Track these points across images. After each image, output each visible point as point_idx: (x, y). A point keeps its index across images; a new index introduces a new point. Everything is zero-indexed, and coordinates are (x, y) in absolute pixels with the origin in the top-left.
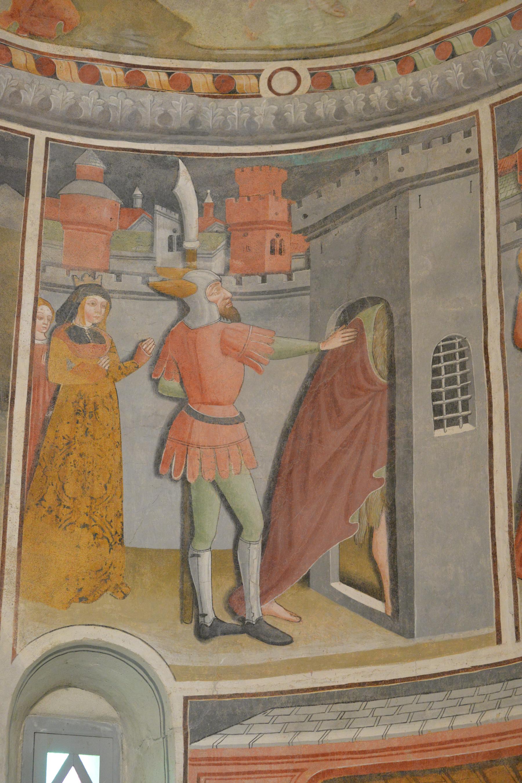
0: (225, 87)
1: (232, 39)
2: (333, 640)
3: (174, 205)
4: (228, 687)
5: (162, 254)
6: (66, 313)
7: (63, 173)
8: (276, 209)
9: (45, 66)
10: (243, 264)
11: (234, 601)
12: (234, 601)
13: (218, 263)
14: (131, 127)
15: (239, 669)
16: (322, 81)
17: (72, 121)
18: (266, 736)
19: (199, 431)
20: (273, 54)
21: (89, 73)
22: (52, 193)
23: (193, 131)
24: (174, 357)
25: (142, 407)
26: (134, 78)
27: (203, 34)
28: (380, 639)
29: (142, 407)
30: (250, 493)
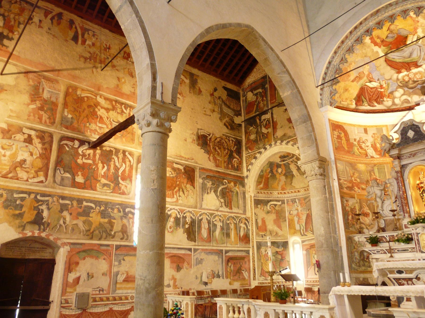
0: (299, 191)
1: (298, 187)
2: (310, 236)
3: (296, 202)
4: (304, 239)
5: (296, 207)
6: (290, 213)
7: (288, 201)
8: (303, 202)
9: (285, 193)
10: (302, 207)
11: (304, 233)
12: (304, 233)
13: (300, 206)
14: (292, 197)
15: (305, 238)
16: (305, 190)
17: (287, 197)
18: (306, 243)
19: (300, 220)
20: (302, 188)
21: (288, 193)
22: (287, 203)
23: (296, 196)
24: (298, 215)
25: (296, 219)
26: (292, 192)
27: (296, 187)
28: (312, 235)
29: (296, 219)
30: (304, 224)
